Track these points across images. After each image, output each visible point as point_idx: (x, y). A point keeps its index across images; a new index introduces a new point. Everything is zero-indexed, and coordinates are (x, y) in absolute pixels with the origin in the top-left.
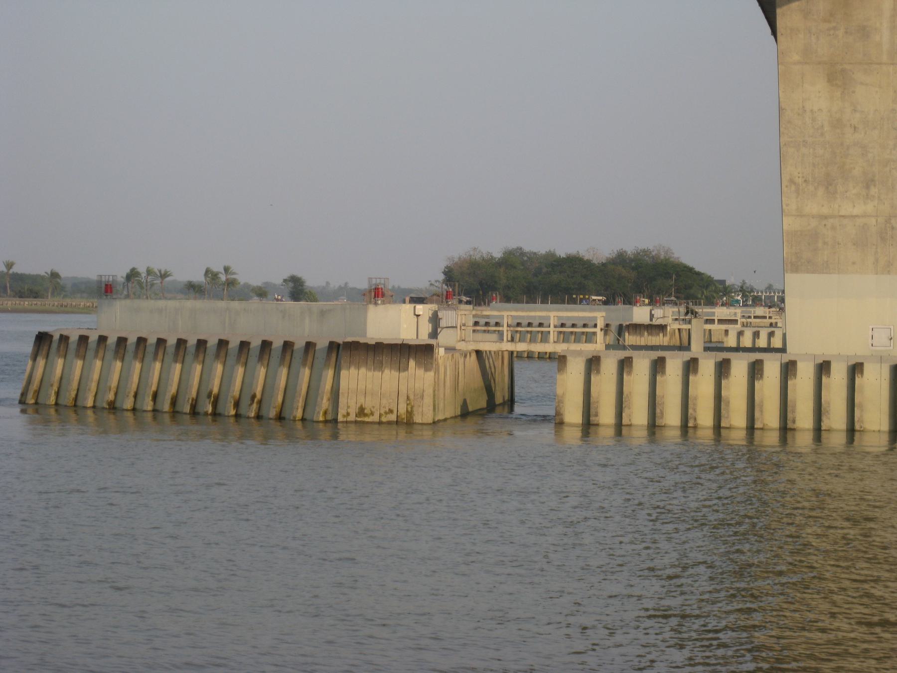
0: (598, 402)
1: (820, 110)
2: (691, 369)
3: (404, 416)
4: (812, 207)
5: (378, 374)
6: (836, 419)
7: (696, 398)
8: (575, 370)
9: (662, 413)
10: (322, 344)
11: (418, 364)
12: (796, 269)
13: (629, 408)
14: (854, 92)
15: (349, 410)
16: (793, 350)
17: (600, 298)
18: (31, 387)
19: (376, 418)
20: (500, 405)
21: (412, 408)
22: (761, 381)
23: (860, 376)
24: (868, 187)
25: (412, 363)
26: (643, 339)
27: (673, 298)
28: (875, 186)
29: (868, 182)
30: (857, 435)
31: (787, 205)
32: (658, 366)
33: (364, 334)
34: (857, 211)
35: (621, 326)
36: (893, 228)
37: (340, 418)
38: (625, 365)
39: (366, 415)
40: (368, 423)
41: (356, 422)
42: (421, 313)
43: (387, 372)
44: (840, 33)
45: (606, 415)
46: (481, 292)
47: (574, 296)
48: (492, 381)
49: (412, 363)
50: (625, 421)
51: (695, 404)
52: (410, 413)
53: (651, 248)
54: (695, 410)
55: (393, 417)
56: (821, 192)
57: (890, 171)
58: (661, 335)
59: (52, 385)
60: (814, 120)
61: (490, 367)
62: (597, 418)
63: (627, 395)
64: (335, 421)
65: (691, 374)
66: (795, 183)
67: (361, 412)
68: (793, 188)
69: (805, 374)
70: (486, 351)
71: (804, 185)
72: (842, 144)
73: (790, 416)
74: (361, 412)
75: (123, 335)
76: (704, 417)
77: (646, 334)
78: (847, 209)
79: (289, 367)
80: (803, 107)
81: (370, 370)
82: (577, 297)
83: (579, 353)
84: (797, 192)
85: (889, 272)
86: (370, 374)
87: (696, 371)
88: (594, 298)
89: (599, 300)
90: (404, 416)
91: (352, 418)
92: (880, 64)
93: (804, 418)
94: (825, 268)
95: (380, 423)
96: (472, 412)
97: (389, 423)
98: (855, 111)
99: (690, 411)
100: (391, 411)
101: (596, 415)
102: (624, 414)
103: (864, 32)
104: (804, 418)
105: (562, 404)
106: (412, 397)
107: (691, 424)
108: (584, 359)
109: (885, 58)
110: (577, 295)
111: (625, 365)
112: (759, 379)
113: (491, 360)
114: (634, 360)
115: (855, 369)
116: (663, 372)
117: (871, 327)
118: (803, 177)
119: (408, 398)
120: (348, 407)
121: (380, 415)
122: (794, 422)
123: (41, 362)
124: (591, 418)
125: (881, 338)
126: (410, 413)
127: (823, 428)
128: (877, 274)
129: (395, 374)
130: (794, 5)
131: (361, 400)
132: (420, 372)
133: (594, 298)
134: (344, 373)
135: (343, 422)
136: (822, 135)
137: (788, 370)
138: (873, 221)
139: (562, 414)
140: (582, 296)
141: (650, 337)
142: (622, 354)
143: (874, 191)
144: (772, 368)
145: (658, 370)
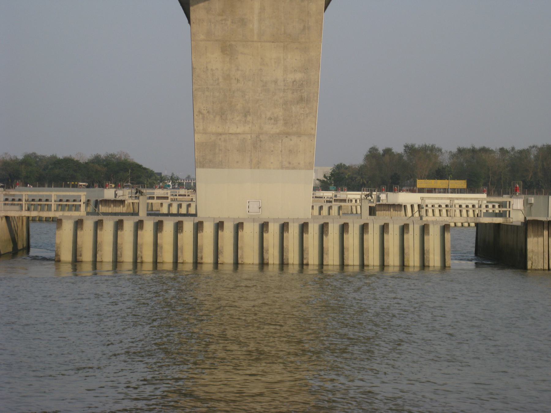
0: (81, 248)
1: (217, 69)
2: (139, 227)
4: (212, 128)
6: (227, 257)
7: (142, 245)
8: (68, 227)
9: (121, 254)
12: (203, 166)
13: (101, 251)
14: (237, 58)
16: (201, 215)
20: (21, 250)
22: (181, 234)
23: (241, 230)
24: (246, 116)
26: (110, 209)
27: (129, 184)
28: (250, 115)
29: (246, 113)
30: (240, 266)
31: (197, 127)
32: (119, 225)
34: (239, 130)
35: (97, 201)
36: (261, 141)
38: (98, 225)
44: (229, 23)
45: (87, 256)
46: (10, 181)
47: (68, 183)
48: (16, 235)
50: (99, 259)
51: (141, 248)
53: (116, 153)
54: (141, 252)
56: (218, 118)
57: (259, 106)
58: (122, 206)
60: (213, 75)
61: (14, 227)
62: (81, 258)
63: (100, 243)
65: (139, 230)
66: (202, 114)
68: (201, 116)
69: (208, 230)
70: (12, 217)
71: (207, 114)
72: (230, 90)
73: (199, 255)
76: (147, 255)
77: (112, 205)
80: (207, 67)
82: (70, 183)
83: (70, 218)
84: (203, 118)
85: (258, 168)
87: (142, 228)
88: (81, 184)
89: (84, 185)
92: (253, 41)
93: (208, 257)
94: (220, 165)
96: (3, 254)
98: (238, 70)
99: (139, 253)
101: (81, 256)
102: (97, 255)
103: (243, 22)
104: (208, 257)
105: (59, 249)
107: (139, 260)
108: (73, 221)
109: (255, 38)
110: (70, 182)
111: (98, 225)
112: (180, 233)
113: (15, 222)
114: (104, 222)
115: (239, 227)
116: (122, 229)
117: (248, 201)
118: (207, 110)
122: (202, 258)
124: (77, 258)
125: (254, 208)
127: (219, 262)
128: (251, 168)
130: (201, 5)
133: (81, 184)
136: (218, 84)
137: (198, 227)
138: (249, 137)
139: (59, 256)
140: (73, 183)
141: (115, 208)
142: (96, 218)
143: (249, 118)
144: (188, 226)
145: (118, 228)
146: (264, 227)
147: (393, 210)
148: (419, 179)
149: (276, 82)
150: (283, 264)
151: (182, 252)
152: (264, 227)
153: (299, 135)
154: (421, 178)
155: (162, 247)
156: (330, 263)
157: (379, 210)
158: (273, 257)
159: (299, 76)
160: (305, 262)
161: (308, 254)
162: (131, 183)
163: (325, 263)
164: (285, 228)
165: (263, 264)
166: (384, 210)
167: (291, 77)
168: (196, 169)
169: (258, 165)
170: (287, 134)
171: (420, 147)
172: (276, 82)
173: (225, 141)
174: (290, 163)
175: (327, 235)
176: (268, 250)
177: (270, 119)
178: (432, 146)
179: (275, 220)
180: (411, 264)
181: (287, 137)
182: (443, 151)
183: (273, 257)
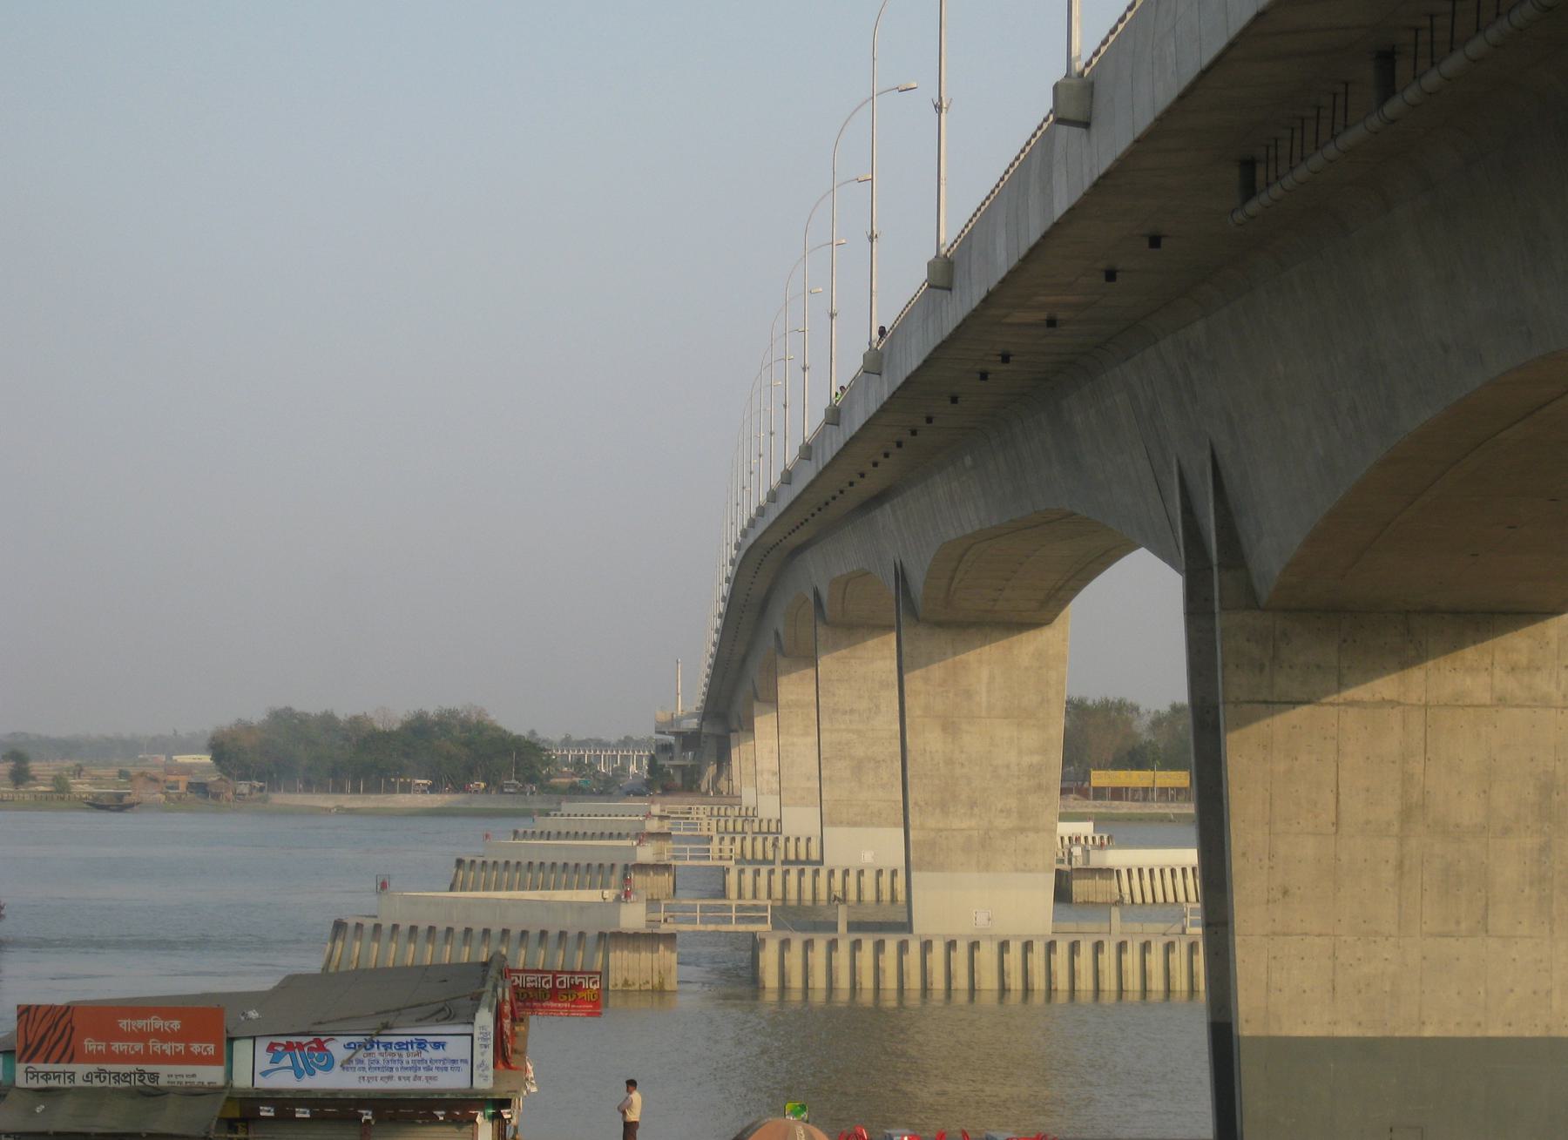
1: (937, 751)
3: (657, 986)
4: (931, 823)
5: (637, 955)
6: (961, 981)
7: (860, 968)
9: (837, 979)
10: (592, 933)
11: (666, 948)
15: (618, 982)
17: (425, 782)
18: (332, 962)
19: (637, 987)
21: (663, 979)
24: (972, 808)
25: (661, 947)
26: (648, 879)
27: (513, 781)
29: (973, 804)
30: (976, 993)
33: (618, 925)
34: (964, 825)
35: (626, 867)
36: (990, 838)
37: (610, 987)
39: (630, 985)
40: (632, 991)
41: (622, 991)
42: (607, 897)
43: (643, 954)
44: (951, 695)
46: (275, 775)
47: (393, 780)
49: (661, 947)
51: (860, 973)
52: (661, 984)
54: (861, 978)
55: (649, 987)
56: (938, 810)
58: (667, 875)
59: (352, 962)
60: (932, 759)
64: (608, 990)
67: (626, 983)
68: (917, 808)
73: (929, 980)
74: (626, 983)
75: (414, 924)
77: (652, 873)
78: (956, 824)
79: (564, 951)
81: (630, 952)
82: (396, 782)
85: (987, 871)
86: (631, 955)
88: (419, 781)
89: (423, 784)
90: (657, 986)
91: (619, 987)
93: (938, 982)
94: (941, 868)
95: (640, 991)
97: (647, 990)
98: (962, 752)
99: (857, 978)
100: (648, 982)
101: (789, 981)
104: (938, 982)
106: (662, 972)
107: (858, 987)
115: (974, 946)
117: (974, 911)
119: (660, 972)
120: (616, 979)
121: (640, 985)
123: (339, 944)
125: (982, 919)
126: (661, 984)
129: (649, 955)
130: (917, 672)
131: (625, 974)
132: (668, 954)
133: (419, 781)
134: (611, 955)
135: (613, 991)
140: (402, 780)
141: (656, 877)
143: (976, 810)
146: (1004, 946)
147: (1100, 878)
148: (1095, 770)
149: (1008, 766)
150: (1027, 990)
151: (908, 977)
152: (1004, 946)
153: (1037, 830)
154: (1099, 768)
155: (884, 971)
156: (1083, 987)
157: (1077, 879)
158: (1015, 982)
159: (1036, 759)
160: (1053, 987)
161: (1056, 978)
162: (516, 779)
163: (1076, 988)
164: (1029, 947)
165: (1003, 990)
166: (1085, 878)
167: (1026, 760)
168: (914, 874)
169: (987, 867)
170: (1022, 830)
171: (1097, 702)
172: (1008, 766)
173: (947, 838)
174: (1025, 865)
175: (1079, 955)
176: (1009, 974)
177: (1002, 811)
178: (1120, 702)
179: (1017, 937)
180: (1178, 988)
181: (1022, 833)
182: (1142, 710)
183: (1015, 982)
